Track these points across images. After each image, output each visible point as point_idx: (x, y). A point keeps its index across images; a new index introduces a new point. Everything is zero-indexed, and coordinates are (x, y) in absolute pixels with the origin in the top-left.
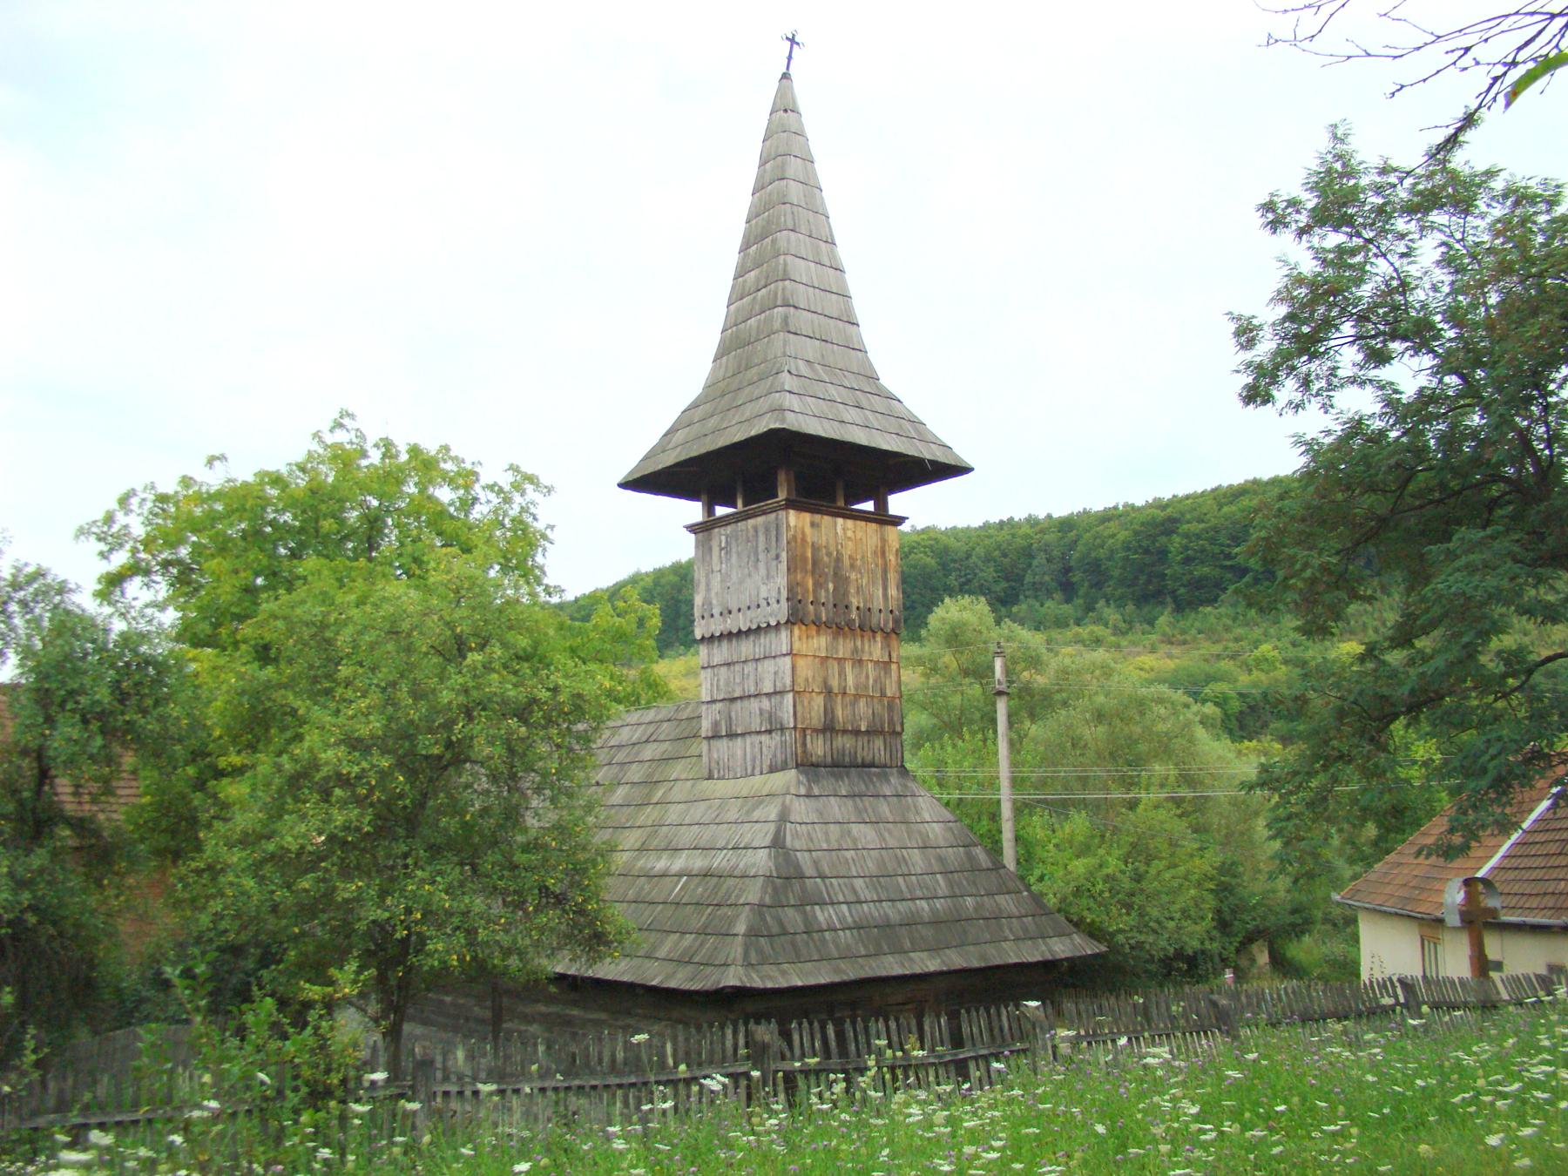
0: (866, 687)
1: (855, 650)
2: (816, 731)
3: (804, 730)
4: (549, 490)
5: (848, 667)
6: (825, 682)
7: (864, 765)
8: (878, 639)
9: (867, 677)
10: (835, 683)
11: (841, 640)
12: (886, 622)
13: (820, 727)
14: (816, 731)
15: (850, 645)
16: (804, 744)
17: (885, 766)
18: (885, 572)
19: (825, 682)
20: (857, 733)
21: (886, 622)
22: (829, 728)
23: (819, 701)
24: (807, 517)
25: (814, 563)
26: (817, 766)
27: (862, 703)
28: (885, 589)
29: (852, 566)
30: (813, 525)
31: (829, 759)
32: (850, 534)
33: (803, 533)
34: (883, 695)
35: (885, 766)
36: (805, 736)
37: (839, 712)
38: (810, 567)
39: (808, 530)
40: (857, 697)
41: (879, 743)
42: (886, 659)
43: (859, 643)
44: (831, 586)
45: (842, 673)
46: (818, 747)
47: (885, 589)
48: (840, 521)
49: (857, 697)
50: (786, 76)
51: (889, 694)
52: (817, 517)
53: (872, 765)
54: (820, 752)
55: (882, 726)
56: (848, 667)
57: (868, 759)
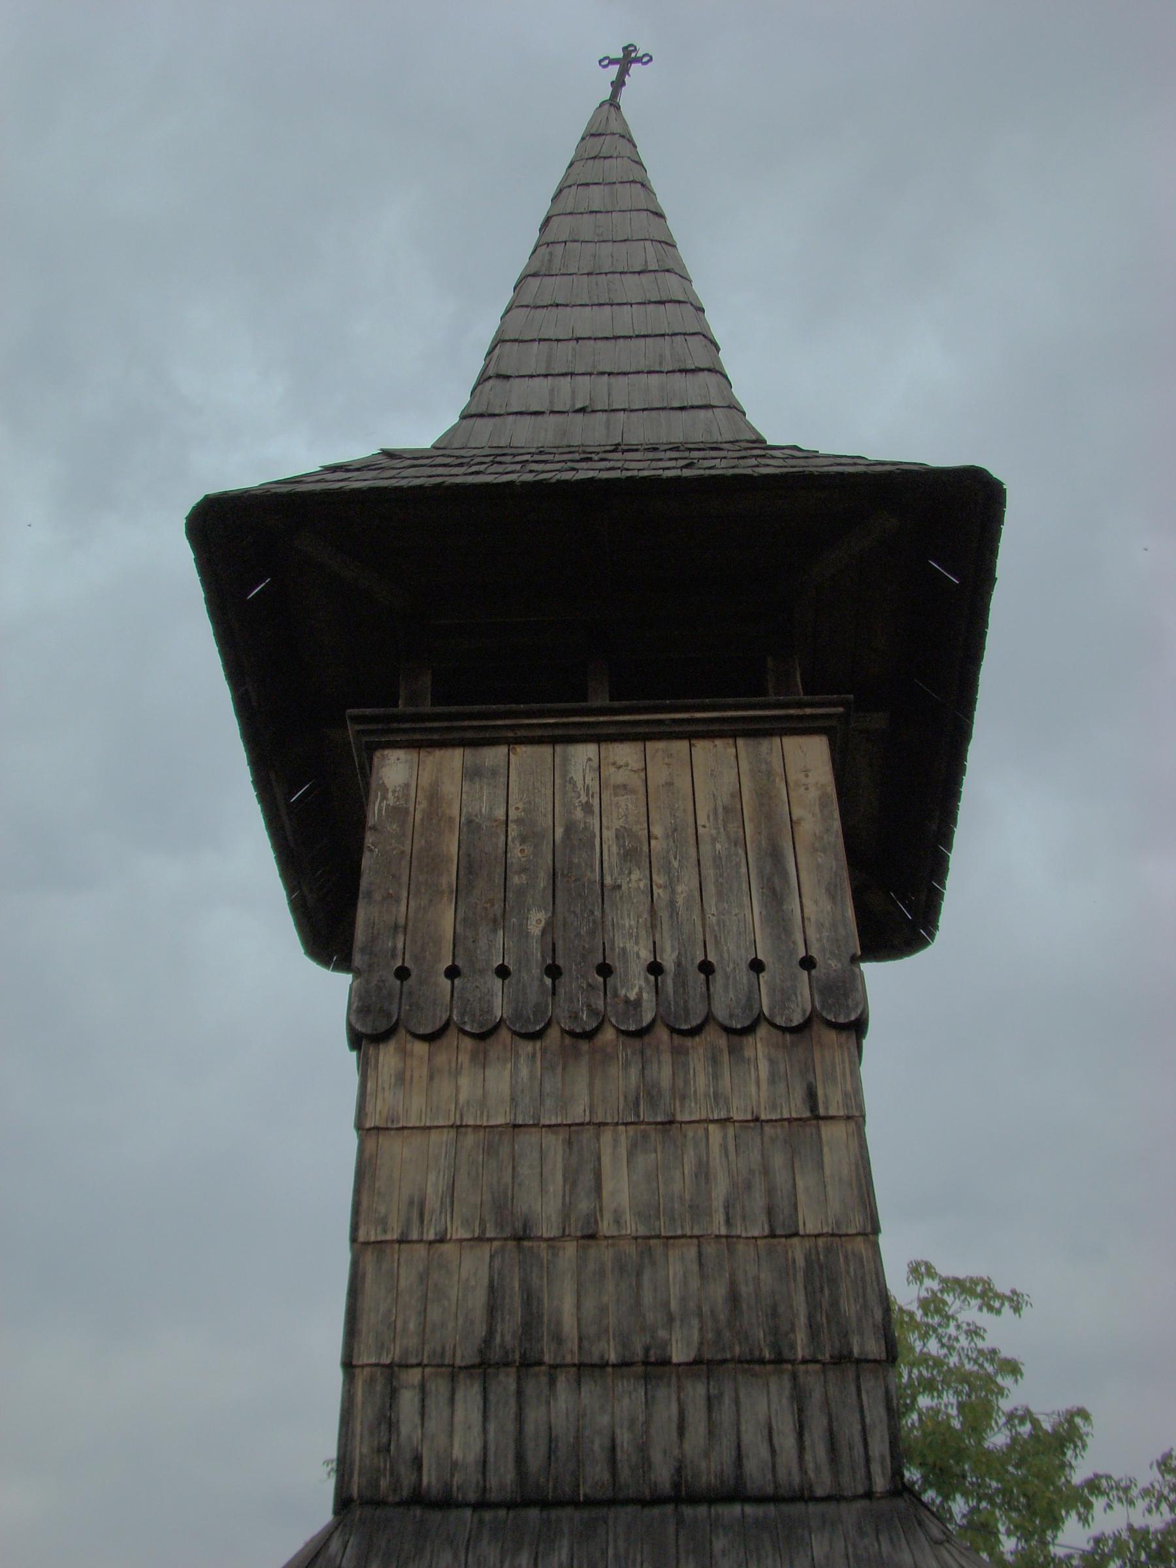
0: (698, 1210)
1: (649, 1093)
2: (454, 1373)
3: (391, 1370)
4: (1016, 1302)
5: (612, 1150)
6: (502, 1206)
7: (683, 1494)
8: (759, 1047)
9: (703, 1172)
10: (545, 1207)
11: (580, 1076)
12: (784, 997)
13: (466, 1354)
14: (454, 1373)
15: (623, 1078)
16: (387, 1421)
17: (804, 1496)
18: (775, 855)
19: (502, 1206)
20: (653, 1367)
21: (784, 997)
22: (510, 1358)
23: (470, 1272)
24: (455, 758)
25: (469, 867)
26: (446, 1502)
27: (677, 1269)
28: (775, 898)
29: (629, 855)
30: (472, 774)
31: (503, 1477)
32: (620, 777)
33: (434, 796)
34: (782, 1230)
35: (804, 1496)
36: (393, 1394)
37: (565, 1305)
38: (449, 878)
39: (451, 787)
40: (653, 1245)
41: (763, 1406)
42: (796, 1108)
43: (663, 1073)
44: (536, 921)
45: (585, 1176)
46: (457, 1435)
47: (775, 898)
48: (583, 754)
49: (653, 1245)
50: (613, 103)
51: (810, 1222)
52: (493, 756)
53: (736, 1494)
54: (465, 1447)
55: (779, 1336)
56: (612, 1150)
57: (710, 1468)
